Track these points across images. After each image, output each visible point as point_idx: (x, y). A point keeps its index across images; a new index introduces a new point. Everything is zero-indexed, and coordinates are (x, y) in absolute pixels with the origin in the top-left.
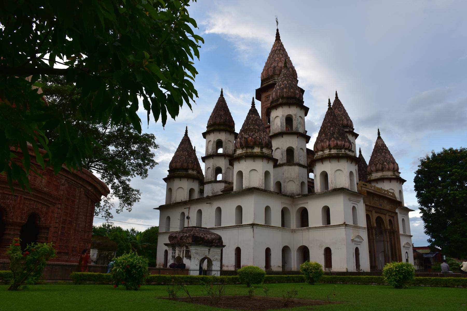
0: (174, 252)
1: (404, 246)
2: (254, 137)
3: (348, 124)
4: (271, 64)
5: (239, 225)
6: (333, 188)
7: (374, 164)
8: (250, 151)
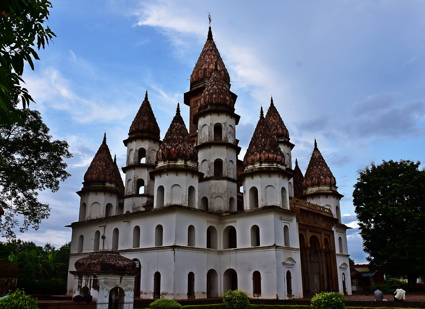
0: (81, 281)
1: (340, 267)
2: (178, 148)
3: (283, 133)
4: (202, 66)
5: (159, 247)
6: (264, 206)
7: (310, 178)
8: (173, 164)
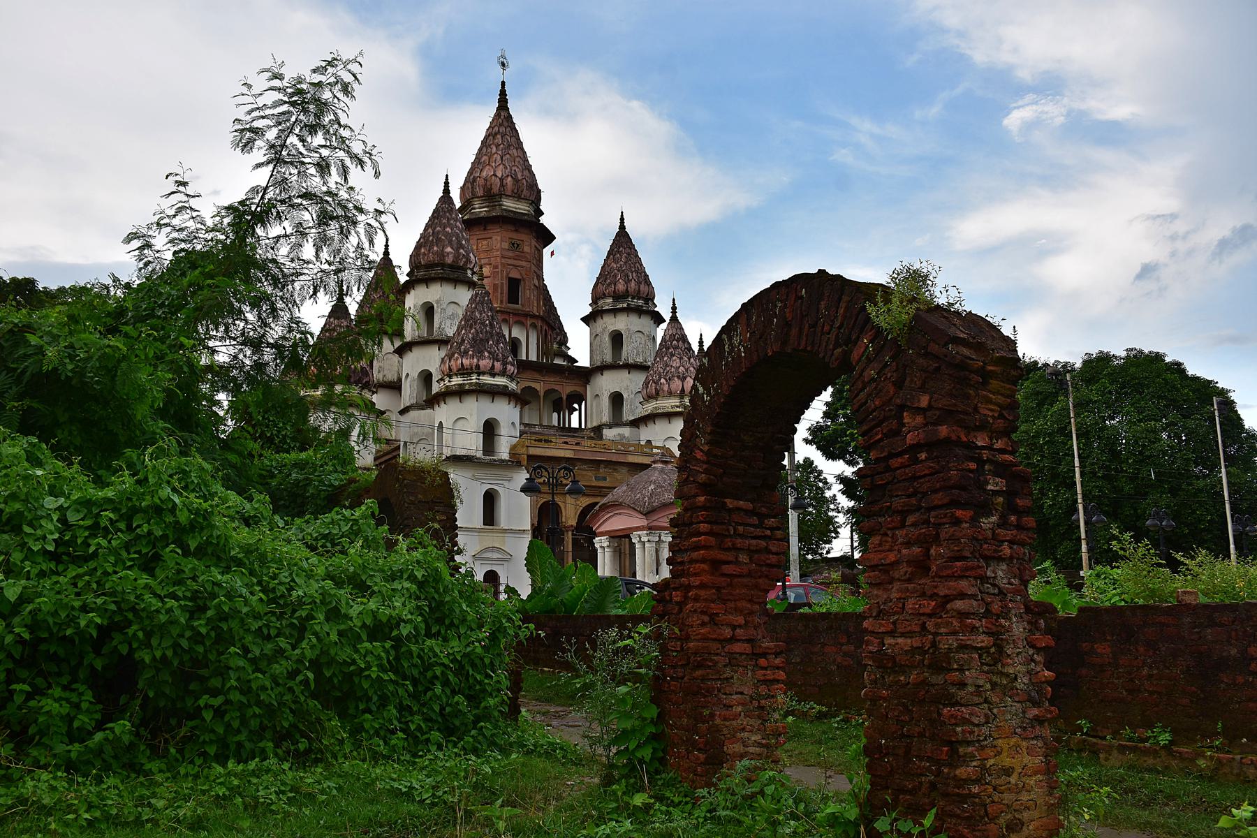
3: (627, 289)
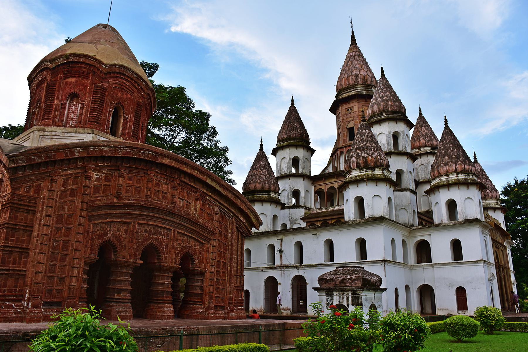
0: (330, 298)
2: (374, 156)
4: (352, 72)
8: (371, 173)
